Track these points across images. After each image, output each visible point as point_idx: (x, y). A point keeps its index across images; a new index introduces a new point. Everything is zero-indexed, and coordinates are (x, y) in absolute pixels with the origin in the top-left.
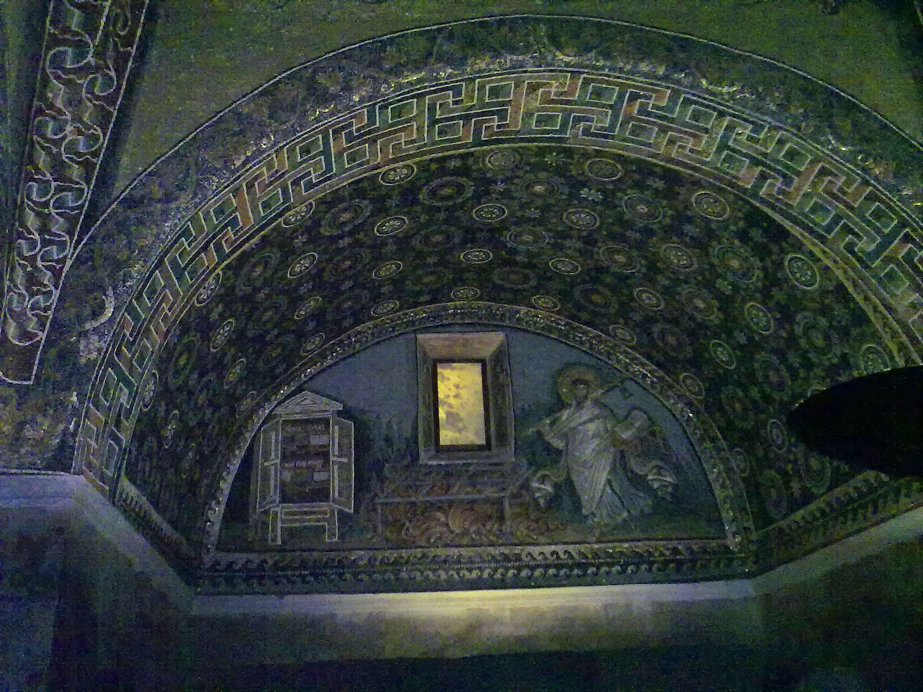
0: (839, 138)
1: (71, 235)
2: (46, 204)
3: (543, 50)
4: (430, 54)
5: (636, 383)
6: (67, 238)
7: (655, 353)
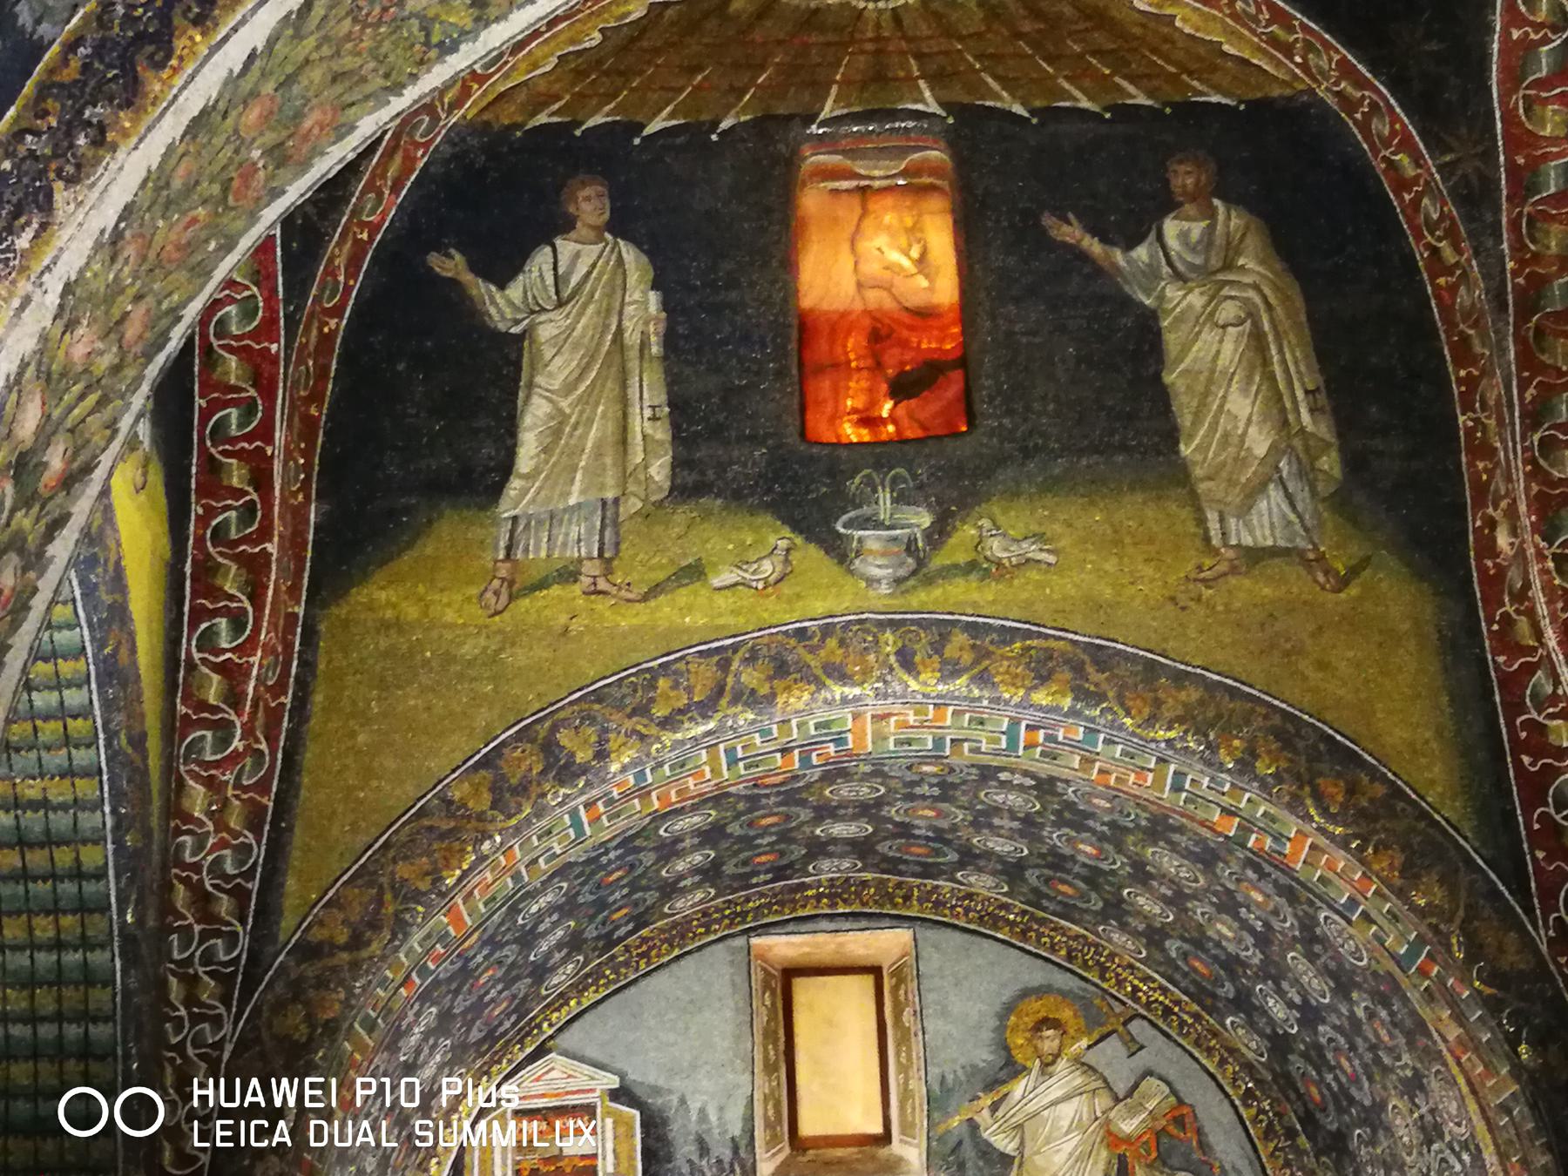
0: (1324, 812)
1: (226, 1000)
2: (188, 962)
3: (889, 678)
4: (720, 690)
5: (1150, 1022)
6: (222, 1010)
7: (1178, 977)
